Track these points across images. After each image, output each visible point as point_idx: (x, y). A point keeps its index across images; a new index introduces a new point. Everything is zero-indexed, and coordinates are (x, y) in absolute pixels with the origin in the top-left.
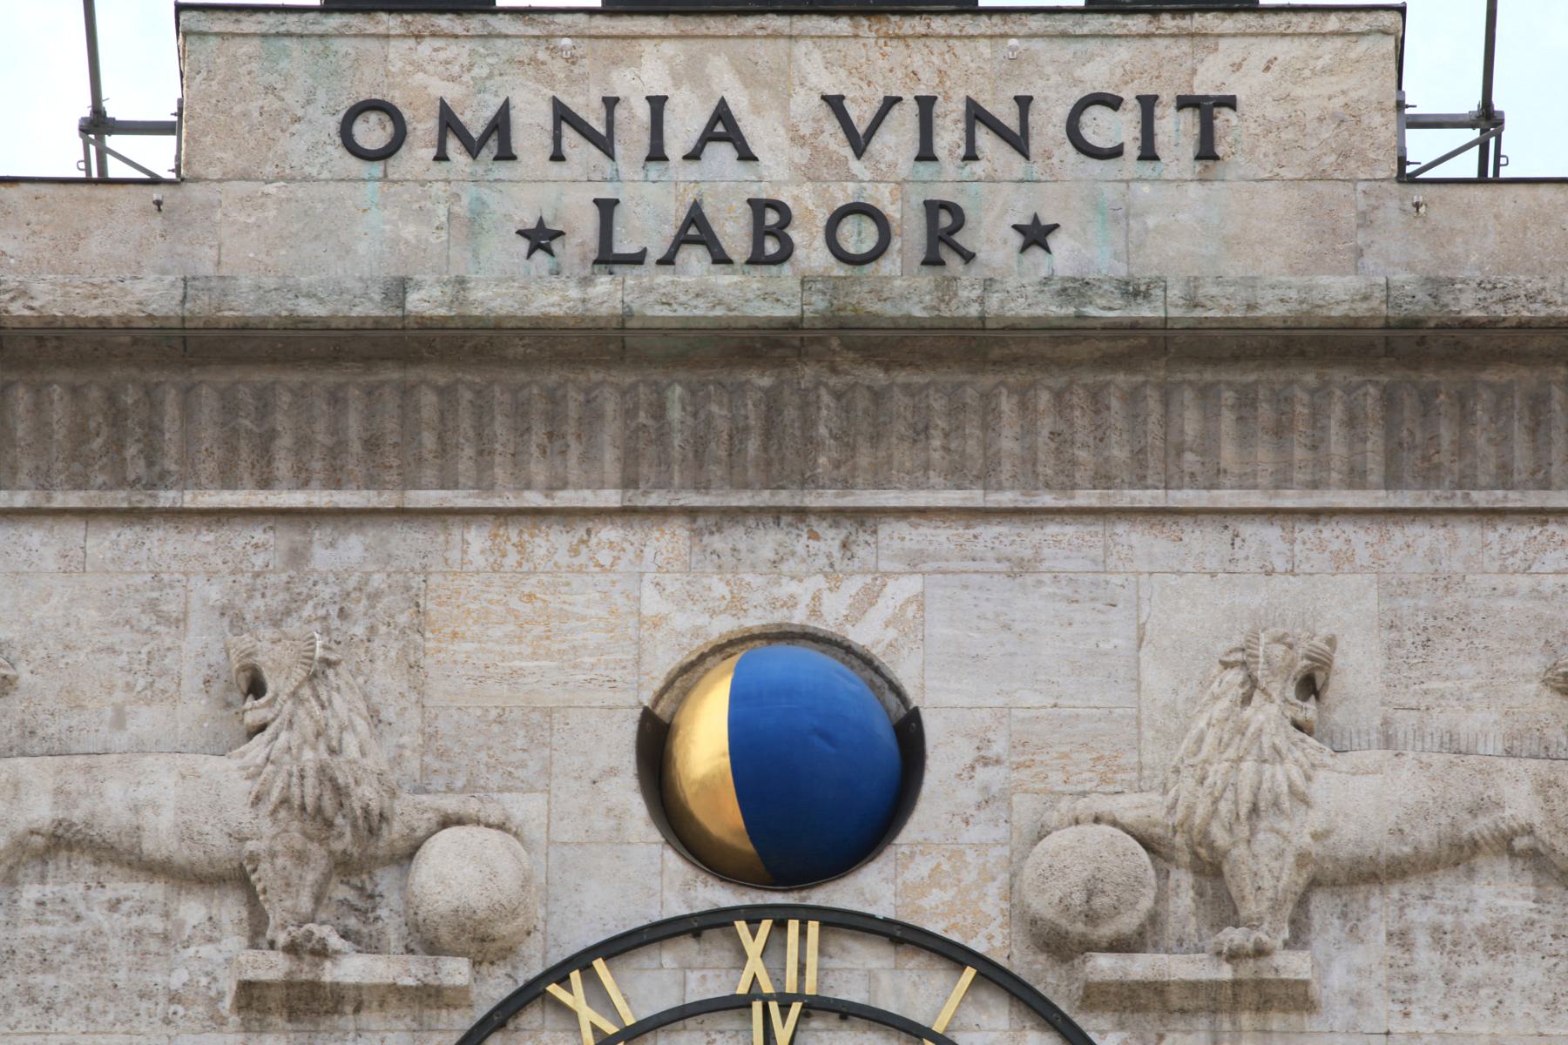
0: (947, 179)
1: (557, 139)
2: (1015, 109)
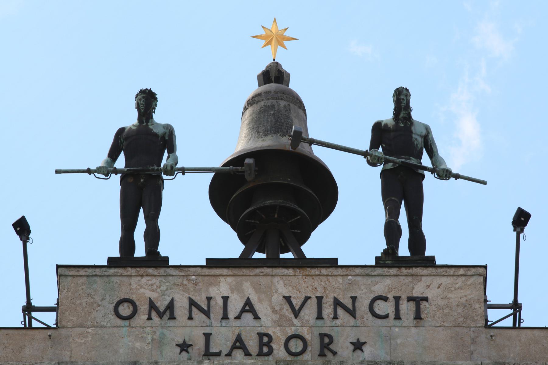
1: (190, 312)
2: (351, 301)
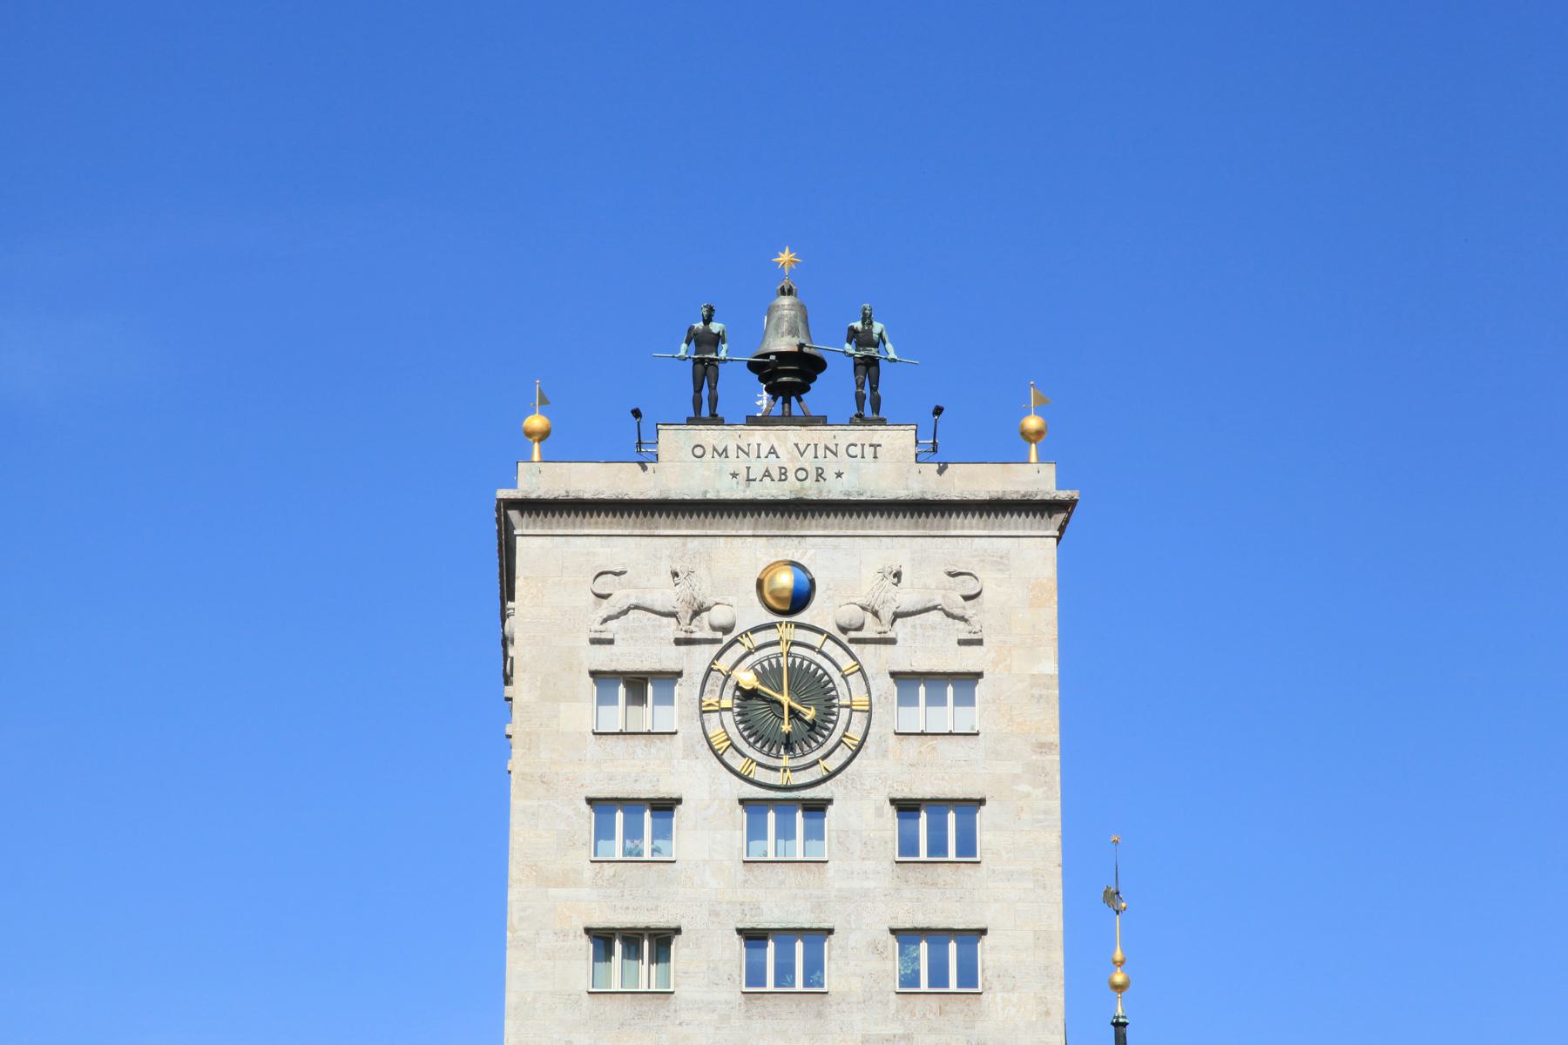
0: (820, 462)
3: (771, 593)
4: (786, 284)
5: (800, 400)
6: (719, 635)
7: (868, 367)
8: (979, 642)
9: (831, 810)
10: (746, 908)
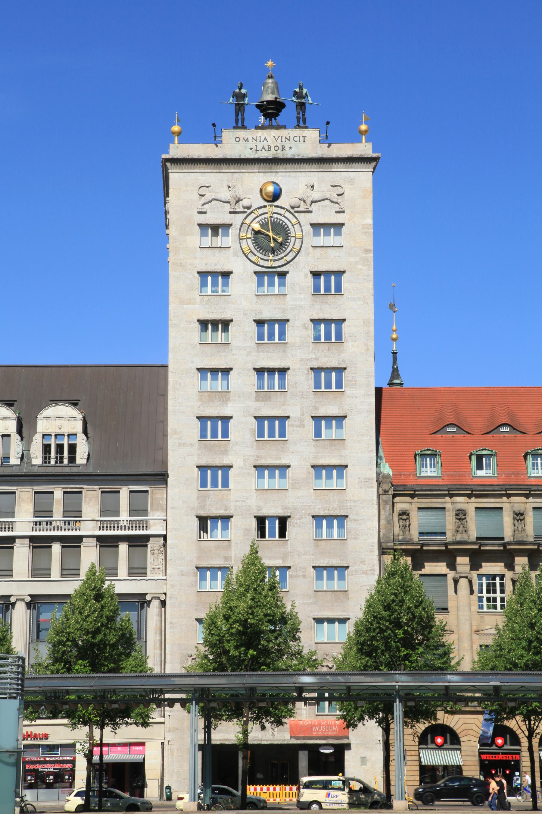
0: (283, 143)
3: (265, 194)
4: (270, 74)
5: (275, 119)
6: (246, 210)
7: (301, 106)
8: (343, 212)
9: (288, 275)
10: (257, 312)
